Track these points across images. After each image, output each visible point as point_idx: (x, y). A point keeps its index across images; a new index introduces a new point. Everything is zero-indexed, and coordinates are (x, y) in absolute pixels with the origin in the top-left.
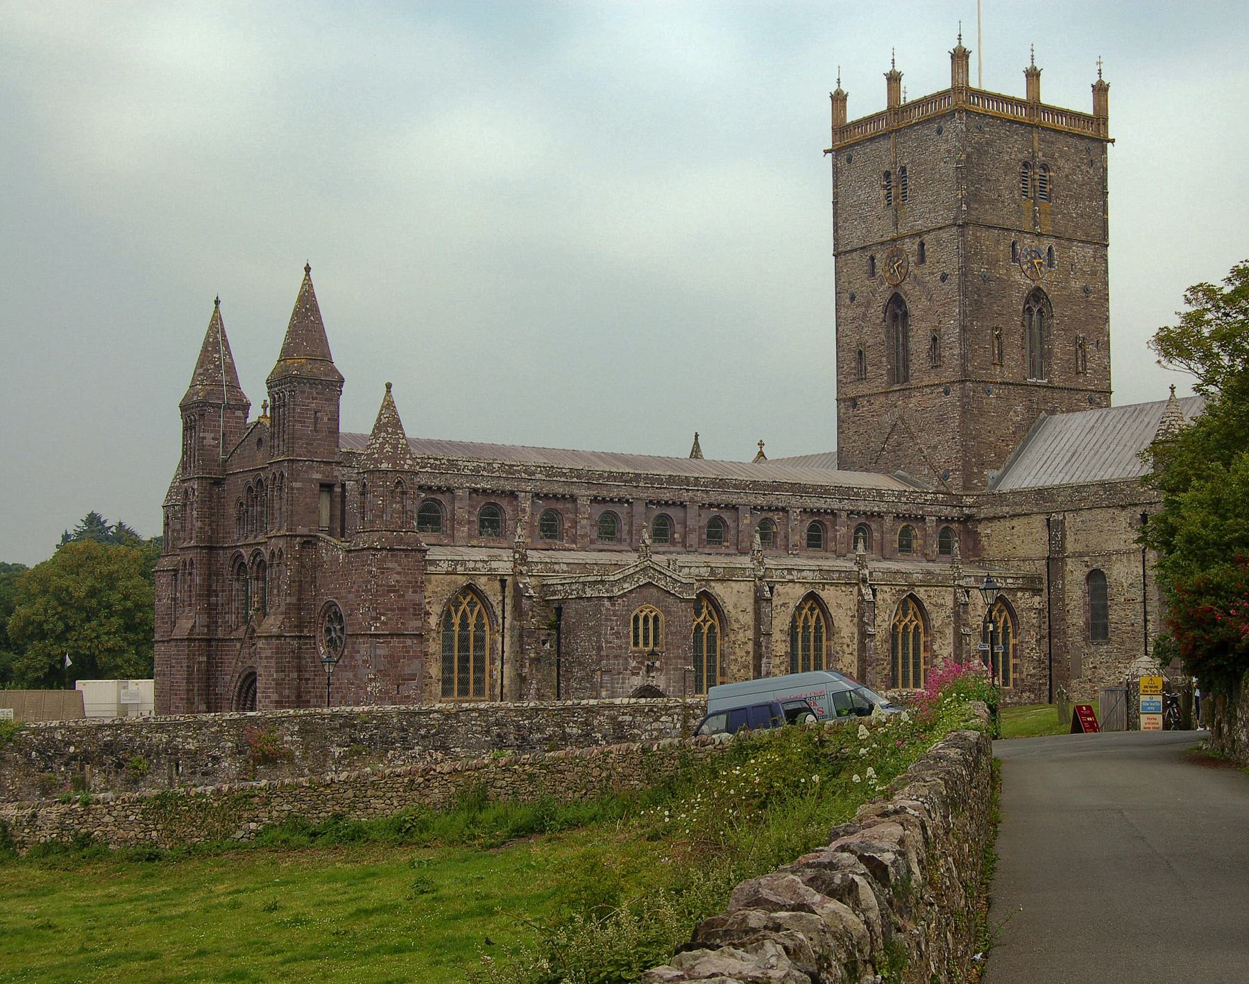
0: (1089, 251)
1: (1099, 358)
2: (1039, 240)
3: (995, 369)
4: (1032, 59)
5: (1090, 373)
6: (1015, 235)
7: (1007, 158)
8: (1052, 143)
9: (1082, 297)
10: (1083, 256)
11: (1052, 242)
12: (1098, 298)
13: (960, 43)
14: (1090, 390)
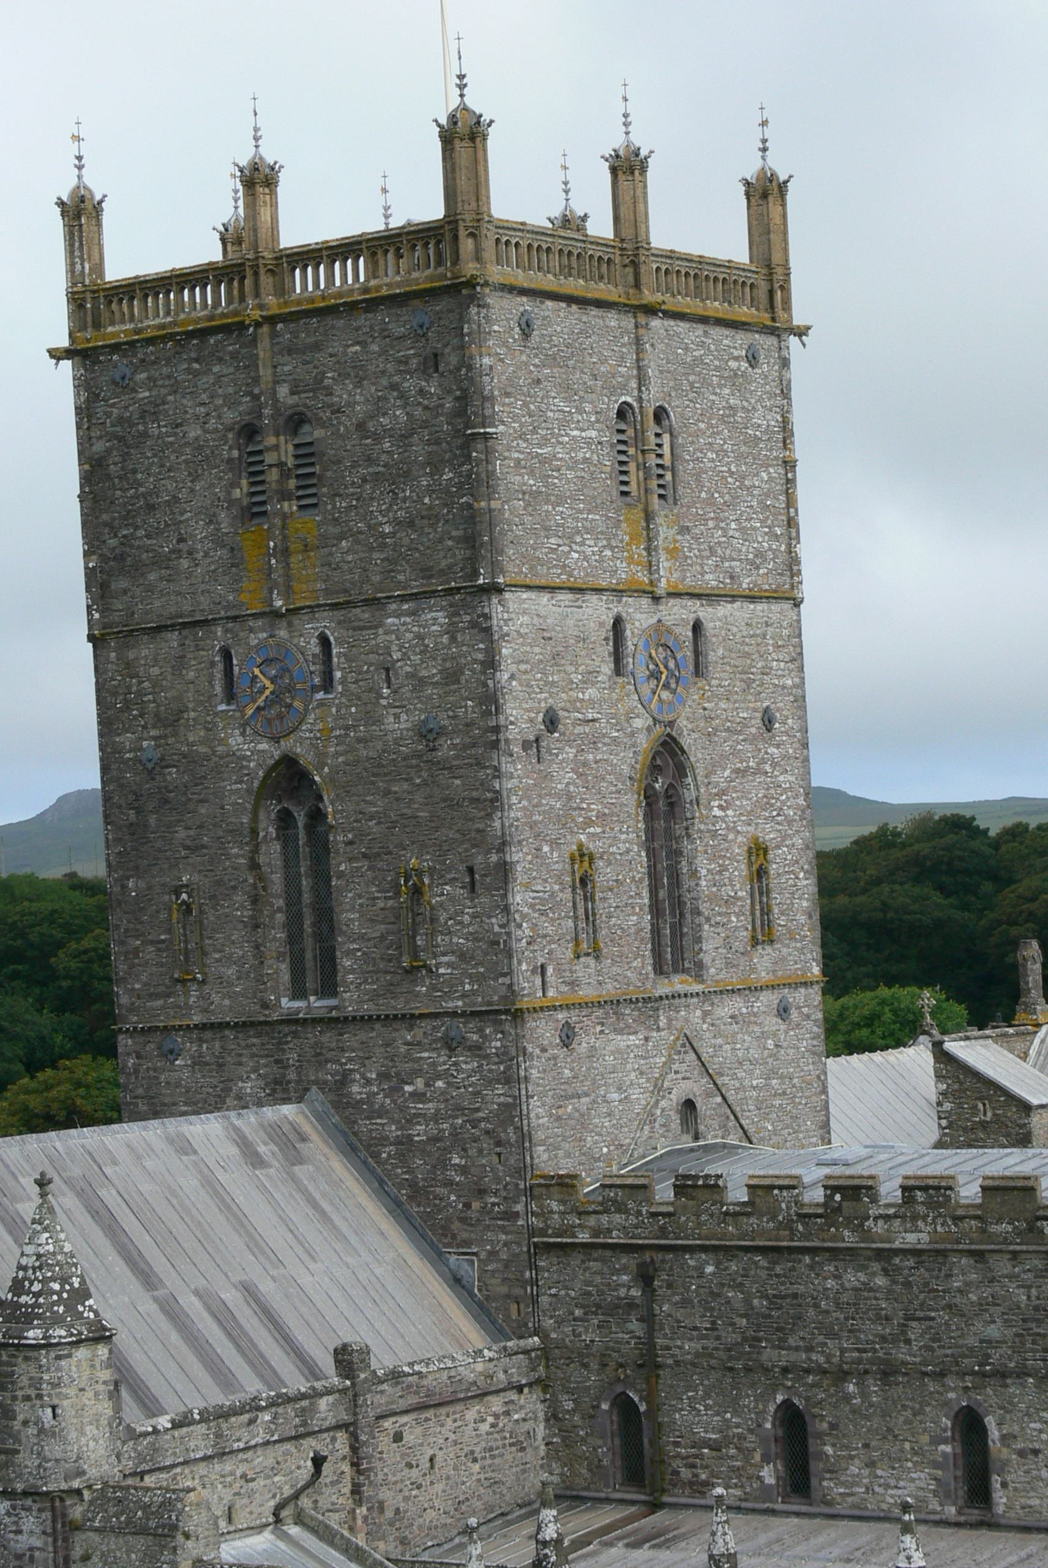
0: (436, 618)
1: (474, 916)
2: (290, 624)
3: (187, 994)
4: (256, 139)
5: (449, 965)
6: (226, 631)
7: (194, 432)
8: (317, 347)
9: (418, 755)
10: (420, 637)
11: (326, 623)
12: (465, 747)
13: (79, 177)
14: (446, 1014)
